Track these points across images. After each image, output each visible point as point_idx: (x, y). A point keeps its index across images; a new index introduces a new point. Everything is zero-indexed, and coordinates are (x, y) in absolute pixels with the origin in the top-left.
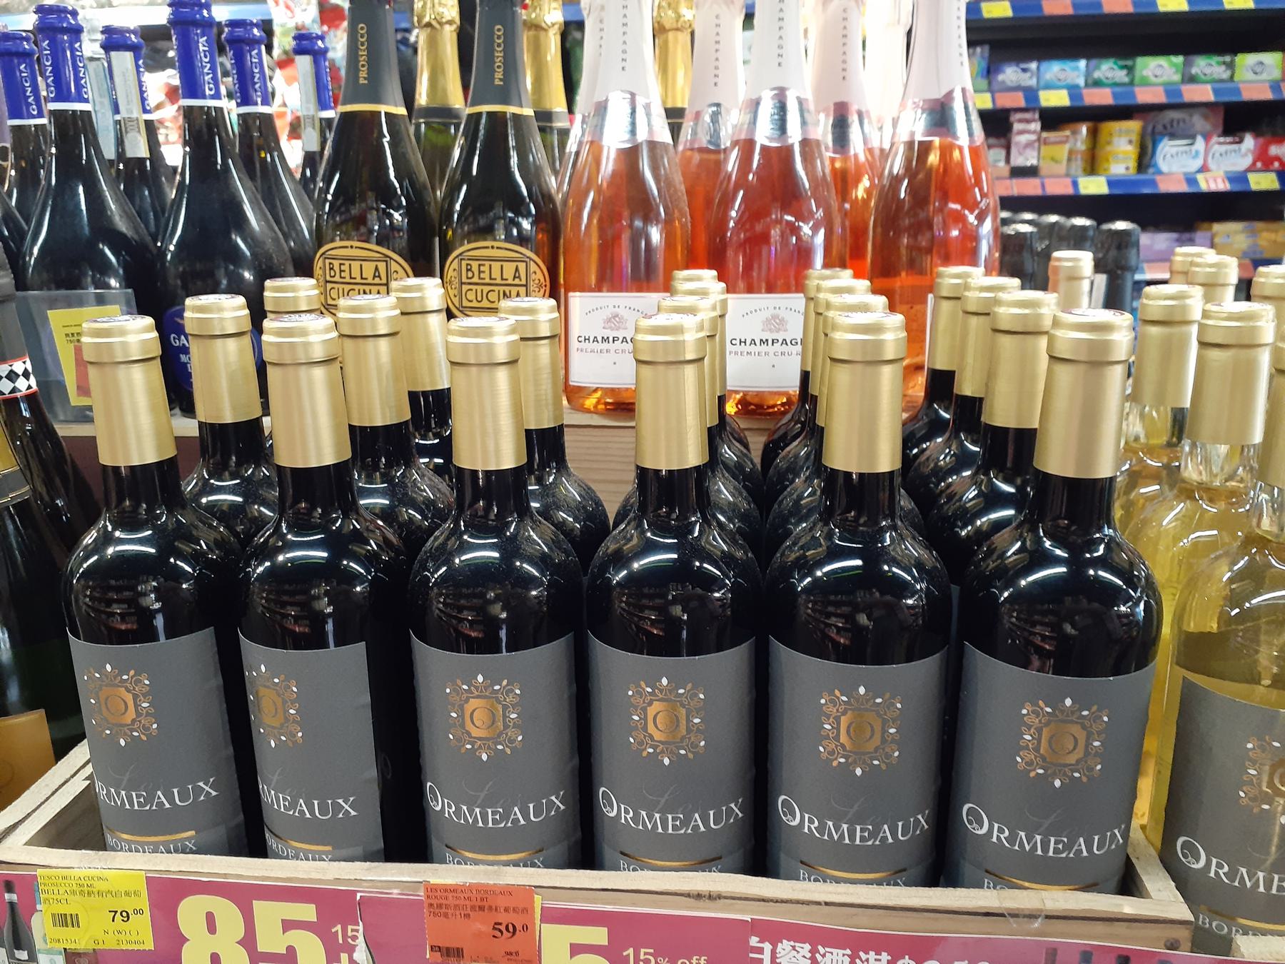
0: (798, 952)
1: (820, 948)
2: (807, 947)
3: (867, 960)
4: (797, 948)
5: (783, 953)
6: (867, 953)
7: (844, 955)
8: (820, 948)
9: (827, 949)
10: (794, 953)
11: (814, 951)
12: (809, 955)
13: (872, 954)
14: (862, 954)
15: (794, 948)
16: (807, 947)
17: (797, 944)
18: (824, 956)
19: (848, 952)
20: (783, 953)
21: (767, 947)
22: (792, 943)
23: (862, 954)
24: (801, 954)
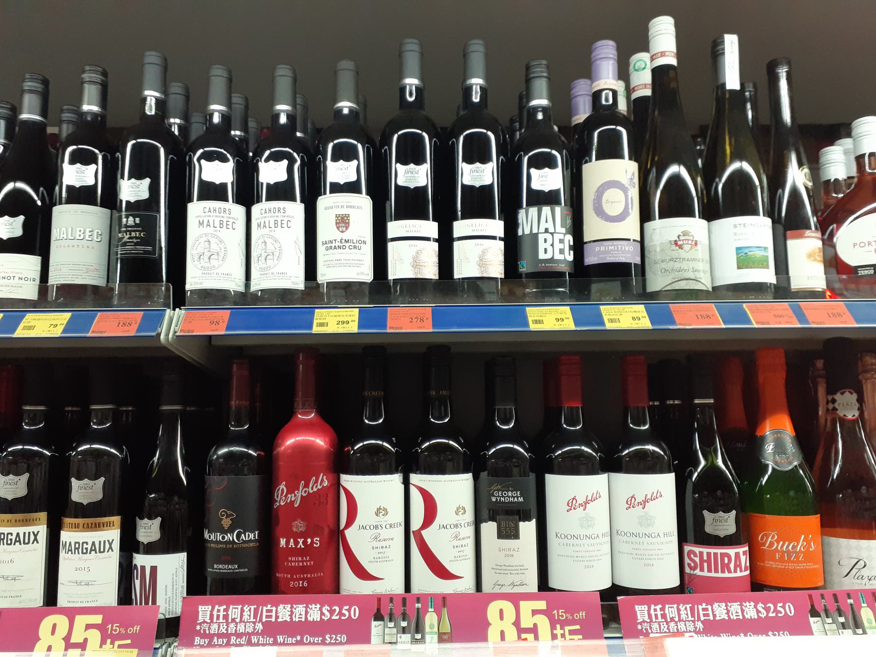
0: (286, 609)
1: (294, 606)
2: (289, 606)
3: (312, 608)
4: (286, 608)
5: (280, 610)
6: (312, 605)
7: (303, 607)
8: (294, 606)
9: (297, 606)
10: (284, 610)
11: (292, 607)
12: (290, 610)
13: (313, 605)
14: (310, 606)
15: (284, 607)
16: (289, 606)
17: (286, 606)
18: (295, 609)
19: (305, 605)
20: (280, 610)
21: (274, 609)
22: (284, 605)
23: (310, 606)
24: (287, 610)
